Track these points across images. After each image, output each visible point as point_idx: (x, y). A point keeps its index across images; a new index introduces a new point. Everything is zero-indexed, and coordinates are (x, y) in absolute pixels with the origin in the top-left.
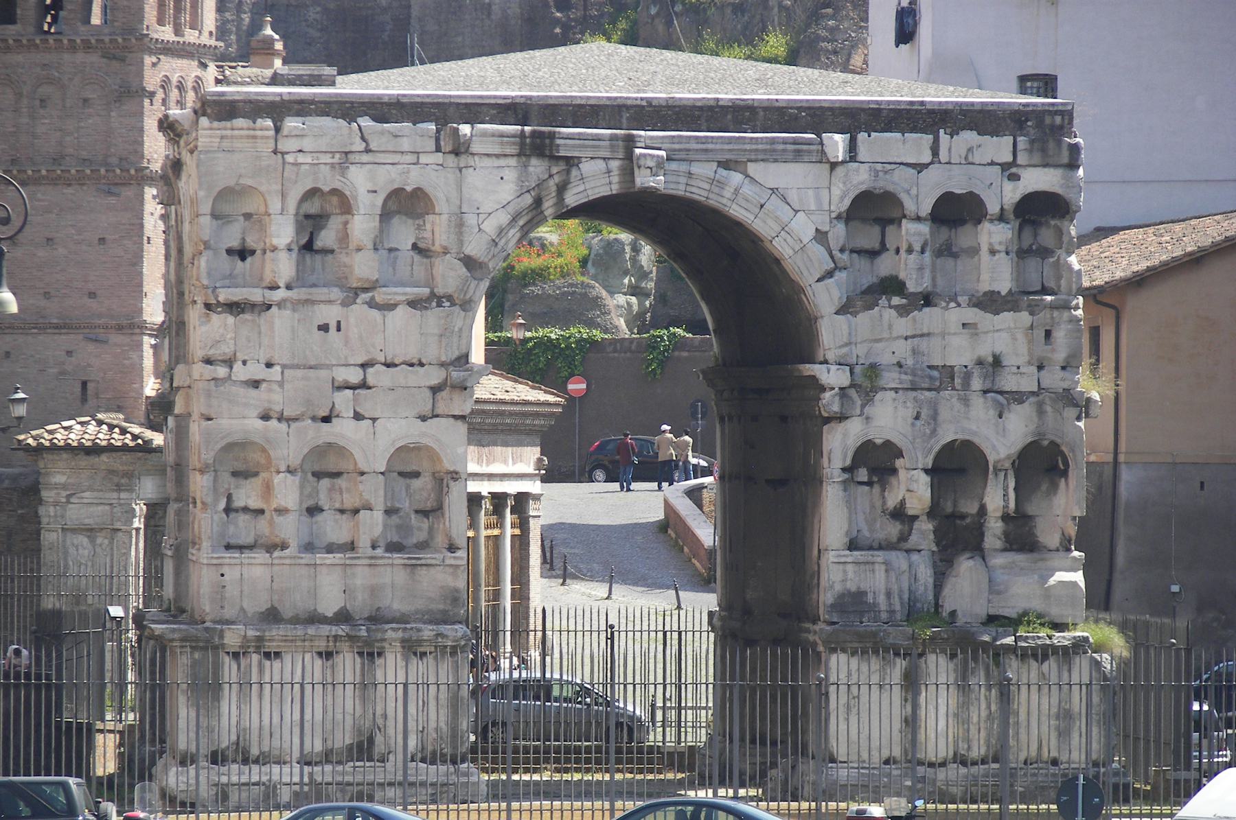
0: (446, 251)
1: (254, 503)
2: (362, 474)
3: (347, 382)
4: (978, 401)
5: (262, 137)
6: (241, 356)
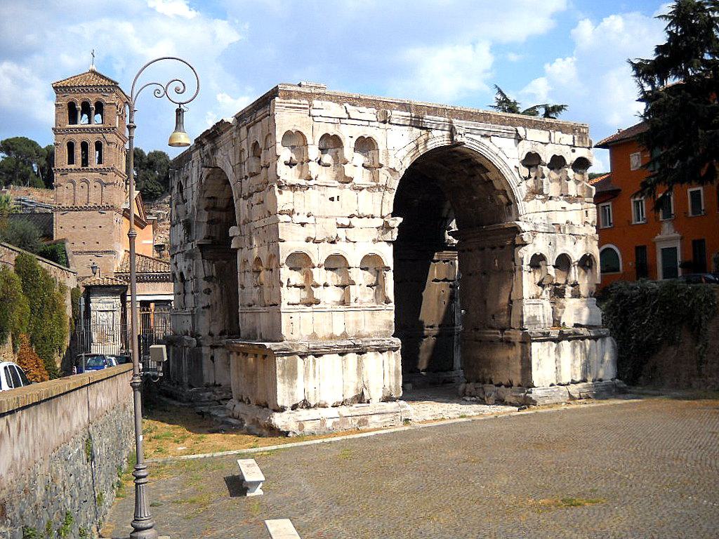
0: (381, 166)
1: (299, 283)
2: (349, 268)
3: (342, 225)
4: (568, 237)
5: (304, 108)
6: (296, 211)
